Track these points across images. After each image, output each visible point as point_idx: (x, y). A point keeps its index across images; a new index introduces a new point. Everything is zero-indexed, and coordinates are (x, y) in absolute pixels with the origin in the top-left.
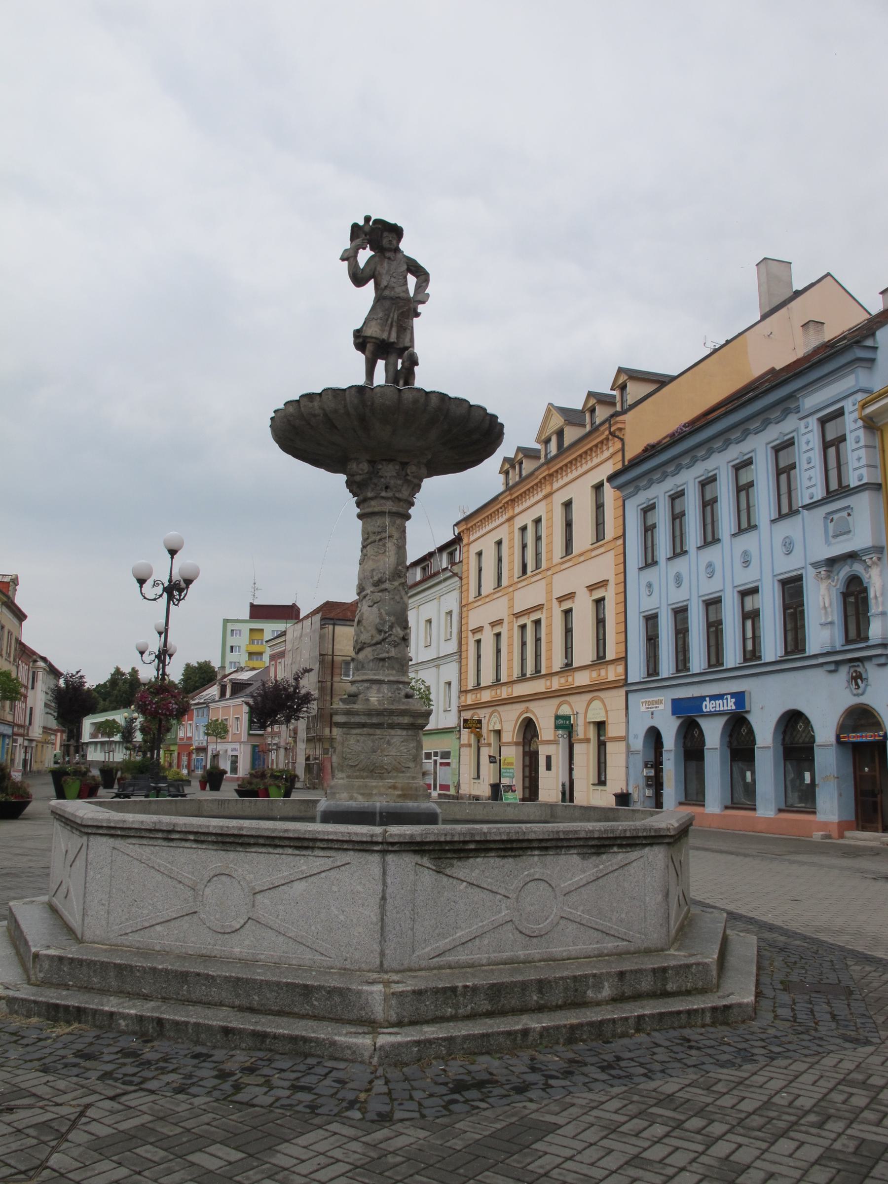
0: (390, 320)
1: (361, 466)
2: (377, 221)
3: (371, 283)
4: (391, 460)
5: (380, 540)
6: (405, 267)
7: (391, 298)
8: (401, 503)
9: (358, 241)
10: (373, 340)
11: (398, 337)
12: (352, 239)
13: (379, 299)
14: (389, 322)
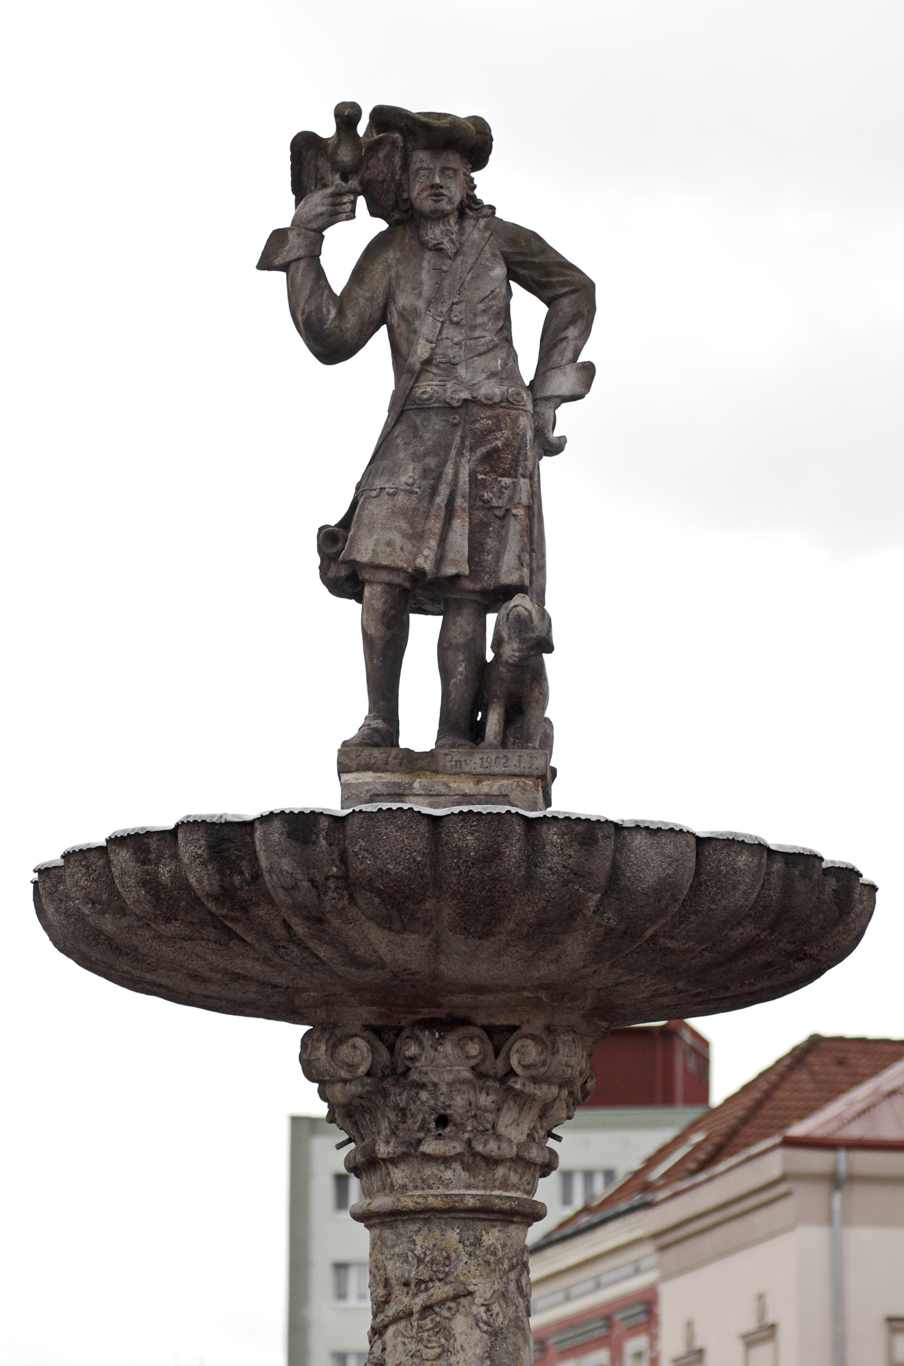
0: (444, 491)
1: (345, 1051)
2: (384, 117)
3: (380, 343)
4: (449, 1024)
5: (427, 1309)
6: (500, 271)
7: (448, 408)
8: (500, 1171)
9: (317, 200)
10: (384, 576)
11: (476, 547)
12: (300, 189)
13: (403, 407)
14: (441, 500)
